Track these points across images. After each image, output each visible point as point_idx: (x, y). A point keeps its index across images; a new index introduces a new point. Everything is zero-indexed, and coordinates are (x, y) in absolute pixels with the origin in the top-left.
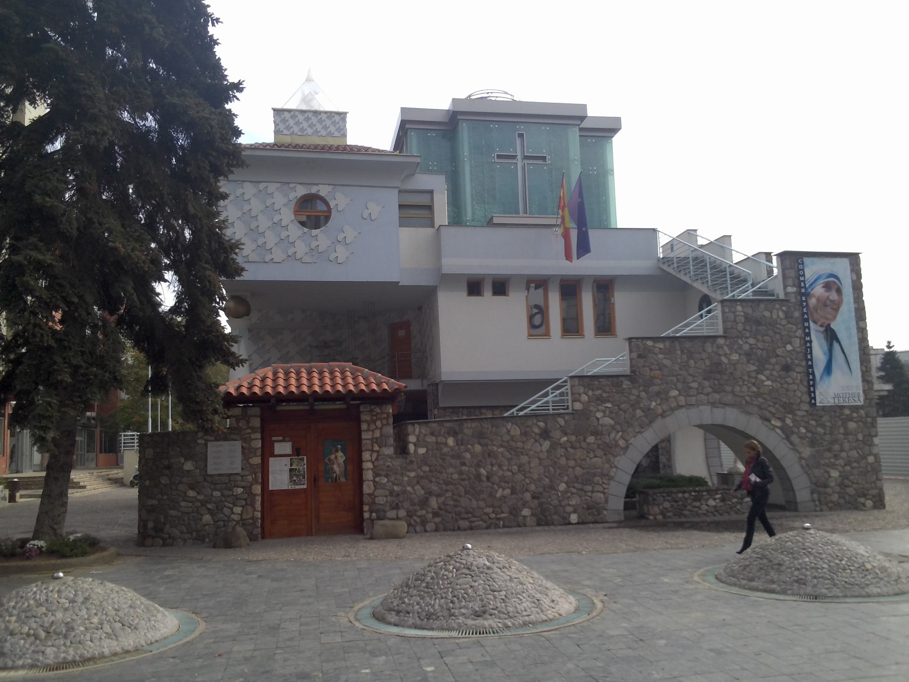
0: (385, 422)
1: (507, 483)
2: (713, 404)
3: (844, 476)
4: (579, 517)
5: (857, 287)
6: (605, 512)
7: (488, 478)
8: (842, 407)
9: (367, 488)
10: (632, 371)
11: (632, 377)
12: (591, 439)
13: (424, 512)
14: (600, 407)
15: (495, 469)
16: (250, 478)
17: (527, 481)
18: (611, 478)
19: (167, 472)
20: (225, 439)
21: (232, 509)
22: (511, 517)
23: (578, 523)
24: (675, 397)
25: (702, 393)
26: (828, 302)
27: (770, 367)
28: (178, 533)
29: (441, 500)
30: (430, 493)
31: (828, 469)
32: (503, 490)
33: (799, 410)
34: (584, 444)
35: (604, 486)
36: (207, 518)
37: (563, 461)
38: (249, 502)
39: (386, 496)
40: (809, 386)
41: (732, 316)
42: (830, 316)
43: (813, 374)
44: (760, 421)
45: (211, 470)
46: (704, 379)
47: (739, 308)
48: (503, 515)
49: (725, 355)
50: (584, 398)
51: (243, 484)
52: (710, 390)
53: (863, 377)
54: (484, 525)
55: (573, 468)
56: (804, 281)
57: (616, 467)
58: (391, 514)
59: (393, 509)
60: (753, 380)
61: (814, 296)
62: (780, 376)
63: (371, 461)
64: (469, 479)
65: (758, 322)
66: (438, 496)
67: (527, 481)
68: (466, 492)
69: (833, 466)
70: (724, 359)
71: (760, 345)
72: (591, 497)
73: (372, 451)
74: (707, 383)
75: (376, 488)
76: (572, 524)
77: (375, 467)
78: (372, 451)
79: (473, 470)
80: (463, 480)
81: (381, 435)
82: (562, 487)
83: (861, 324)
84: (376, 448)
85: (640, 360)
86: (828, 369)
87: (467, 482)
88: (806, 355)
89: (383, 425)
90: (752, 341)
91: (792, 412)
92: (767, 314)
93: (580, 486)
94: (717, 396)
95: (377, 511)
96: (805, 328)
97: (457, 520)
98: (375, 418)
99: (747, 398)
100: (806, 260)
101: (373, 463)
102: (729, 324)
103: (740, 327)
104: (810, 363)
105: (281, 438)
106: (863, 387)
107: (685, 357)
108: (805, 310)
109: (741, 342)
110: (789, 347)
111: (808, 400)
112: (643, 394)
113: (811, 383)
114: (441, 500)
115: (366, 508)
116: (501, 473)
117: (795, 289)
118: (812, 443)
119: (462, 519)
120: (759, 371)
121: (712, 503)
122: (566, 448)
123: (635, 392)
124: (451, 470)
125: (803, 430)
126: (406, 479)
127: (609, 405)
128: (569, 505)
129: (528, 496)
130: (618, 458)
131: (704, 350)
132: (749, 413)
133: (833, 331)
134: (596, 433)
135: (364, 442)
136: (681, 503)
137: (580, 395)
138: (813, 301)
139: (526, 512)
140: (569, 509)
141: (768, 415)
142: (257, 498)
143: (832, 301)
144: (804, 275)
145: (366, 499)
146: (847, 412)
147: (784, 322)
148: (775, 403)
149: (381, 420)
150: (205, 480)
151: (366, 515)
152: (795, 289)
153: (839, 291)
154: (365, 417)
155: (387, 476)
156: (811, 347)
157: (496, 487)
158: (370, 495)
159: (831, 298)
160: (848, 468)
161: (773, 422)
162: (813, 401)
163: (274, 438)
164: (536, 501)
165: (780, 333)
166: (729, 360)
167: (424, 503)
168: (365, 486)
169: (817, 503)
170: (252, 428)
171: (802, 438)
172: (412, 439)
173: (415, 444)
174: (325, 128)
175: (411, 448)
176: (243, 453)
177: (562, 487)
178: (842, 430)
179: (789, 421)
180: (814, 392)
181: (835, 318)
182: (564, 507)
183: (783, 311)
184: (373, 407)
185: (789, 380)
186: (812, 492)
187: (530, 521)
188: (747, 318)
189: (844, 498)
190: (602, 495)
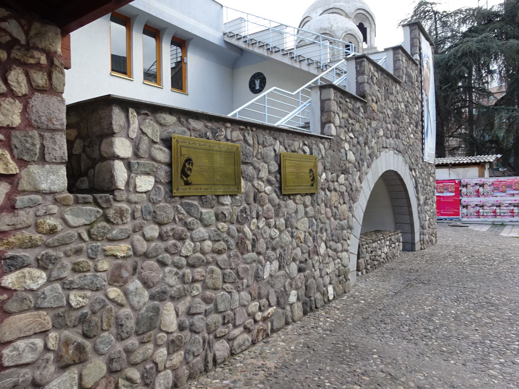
0: (40, 79)
1: (274, 249)
29: (182, 306)
39: (44, 333)
59: (64, 367)
89: (34, 89)
114: (182, 306)
121: (386, 250)
124: (201, 231)
126: (105, 265)
127: (351, 135)
167: (149, 324)
172: (122, 147)
173: (129, 166)
175: (120, 173)
187: (298, 311)
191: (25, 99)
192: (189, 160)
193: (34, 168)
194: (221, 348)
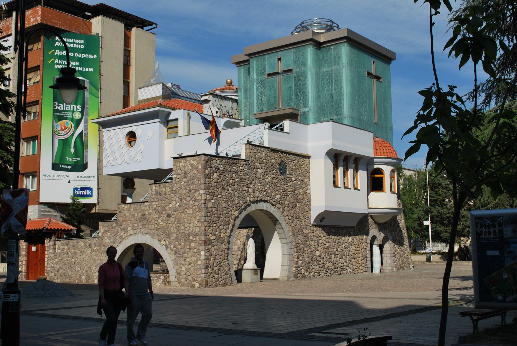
3: (188, 270)
31: (181, 266)
47: (154, 187)
52: (141, 227)
60: (156, 222)
69: (183, 264)
70: (147, 213)
74: (140, 224)
91: (169, 237)
94: (143, 230)
110: (171, 206)
118: (176, 253)
120: (159, 218)
125: (172, 246)
129: (84, 271)
139: (83, 277)
145: (45, 268)
151: (45, 274)
160: (190, 266)
167: (58, 271)
174: (155, 92)
185: (169, 222)
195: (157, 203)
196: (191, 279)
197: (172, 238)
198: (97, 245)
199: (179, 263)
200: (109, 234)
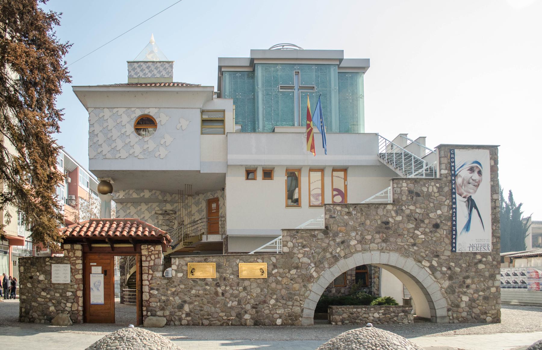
0: (156, 256)
2: (382, 250)
3: (472, 300)
4: (283, 321)
5: (494, 170)
6: (300, 319)
7: (223, 294)
8: (475, 254)
9: (146, 297)
10: (327, 227)
11: (326, 231)
12: (293, 272)
13: (181, 313)
14: (301, 251)
15: (227, 288)
16: (76, 286)
17: (249, 297)
18: (307, 298)
19: (30, 280)
20: (61, 263)
21: (66, 304)
22: (238, 319)
23: (282, 325)
24: (354, 245)
25: (374, 243)
26: (471, 181)
27: (424, 226)
28: (36, 315)
30: (185, 302)
32: (233, 302)
33: (443, 255)
34: (288, 275)
35: (301, 302)
36: (52, 308)
37: (273, 285)
38: (75, 300)
40: (452, 239)
41: (399, 190)
42: (471, 191)
43: (456, 230)
44: (414, 263)
45: (54, 281)
46: (376, 233)
47: (404, 185)
48: (232, 318)
49: (392, 217)
50: (290, 244)
51: (72, 290)
53: (492, 233)
54: (219, 323)
55: (281, 290)
56: (454, 166)
57: (311, 291)
58: (159, 313)
61: (460, 176)
62: (431, 232)
63: (148, 280)
64: (210, 294)
65: (418, 195)
66: (190, 303)
67: (249, 297)
68: (208, 302)
69: (465, 293)
70: (391, 220)
71: (418, 211)
72: (291, 309)
73: (149, 274)
74: (377, 236)
75: (150, 297)
76: (276, 325)
77: (150, 284)
78: (149, 274)
79: (213, 289)
80: (206, 294)
81: (155, 265)
82: (272, 302)
83: (495, 197)
84: (151, 272)
85: (331, 219)
86: (467, 227)
87: (208, 296)
88: (452, 217)
90: (412, 207)
91: (437, 256)
92: (425, 189)
93: (284, 302)
94: (384, 245)
95: (151, 311)
96: (453, 198)
97: (202, 319)
98: (150, 253)
99: (406, 246)
100: (457, 151)
101: (149, 281)
102: (396, 196)
103: (404, 198)
104: (454, 223)
105: (95, 264)
106: (493, 240)
107: (363, 218)
108: (453, 186)
109: (404, 208)
110: (439, 212)
111: (450, 248)
112: (332, 243)
113: (454, 236)
114: (191, 306)
115: (144, 309)
116: (231, 291)
117: (446, 172)
118: (450, 278)
119: (206, 319)
120: (417, 228)
122: (276, 277)
123: (327, 241)
124: (198, 288)
125: (444, 269)
128: (276, 313)
129: (248, 307)
130: (312, 284)
131: (377, 213)
132: (408, 257)
133: (473, 201)
134: (297, 268)
135: (143, 268)
136: (355, 315)
137: (287, 242)
138: (459, 181)
139: (247, 316)
140: (276, 316)
141: (420, 258)
142: (80, 298)
143: (473, 180)
144: (454, 162)
146: (479, 257)
147: (437, 195)
148: (426, 251)
149: (154, 254)
150: (51, 286)
151: (145, 313)
152: (446, 172)
153: (480, 173)
154: (144, 252)
155: (157, 290)
156: (456, 212)
157: (227, 300)
158: (147, 301)
159: (473, 178)
161: (423, 263)
162: (454, 249)
163: (91, 264)
164: (254, 310)
165: (433, 203)
166: (395, 220)
167: (181, 307)
168: (144, 296)
169: (451, 317)
170: (77, 257)
171: (444, 274)
176: (71, 272)
177: (272, 302)
178: (474, 270)
179: (435, 263)
180: (455, 243)
181: (475, 192)
182: (273, 315)
183: (437, 187)
184: (149, 246)
186: (449, 310)
188: (410, 192)
189: (471, 315)
190: (299, 308)
191: (154, 260)
192: (193, 269)
193: (156, 273)
194: (206, 322)
195: (412, 207)
196: (479, 312)
197: (442, 257)
198: (278, 265)
199: (457, 290)
200: (306, 249)
